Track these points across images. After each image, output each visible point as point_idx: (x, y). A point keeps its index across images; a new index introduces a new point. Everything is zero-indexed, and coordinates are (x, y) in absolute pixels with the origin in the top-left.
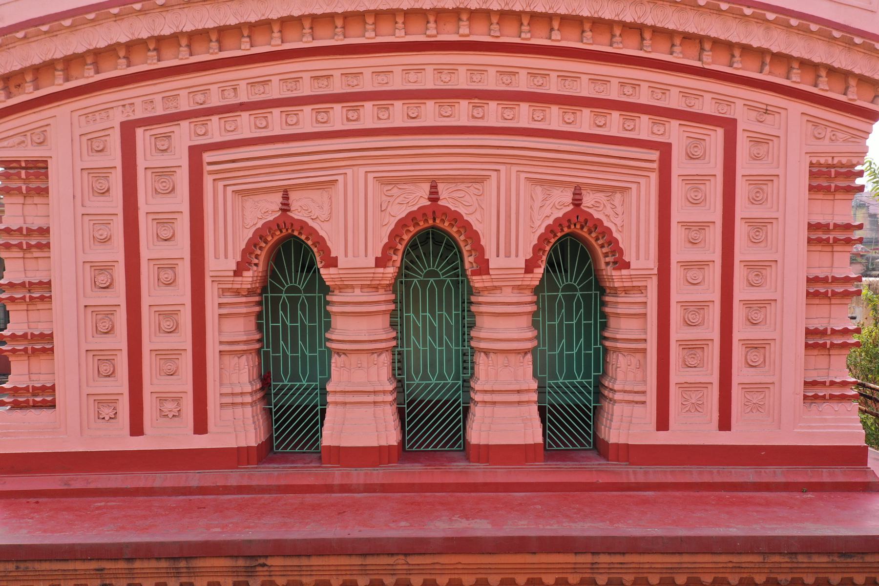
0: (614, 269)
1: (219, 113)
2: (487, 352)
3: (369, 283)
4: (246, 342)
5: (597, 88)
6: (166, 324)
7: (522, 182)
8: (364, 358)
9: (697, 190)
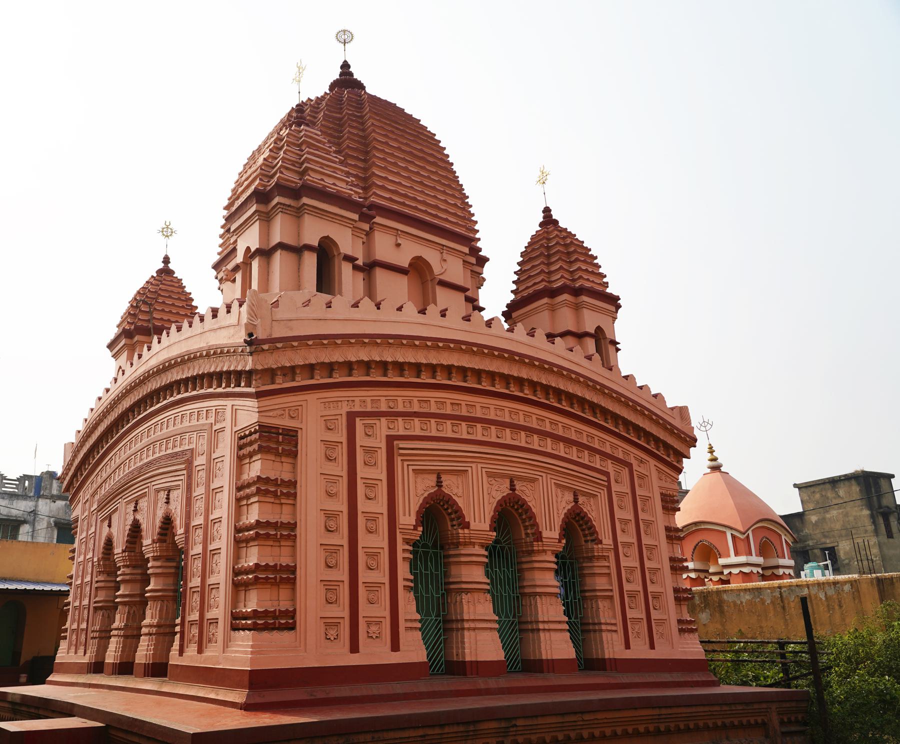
2: (540, 594)
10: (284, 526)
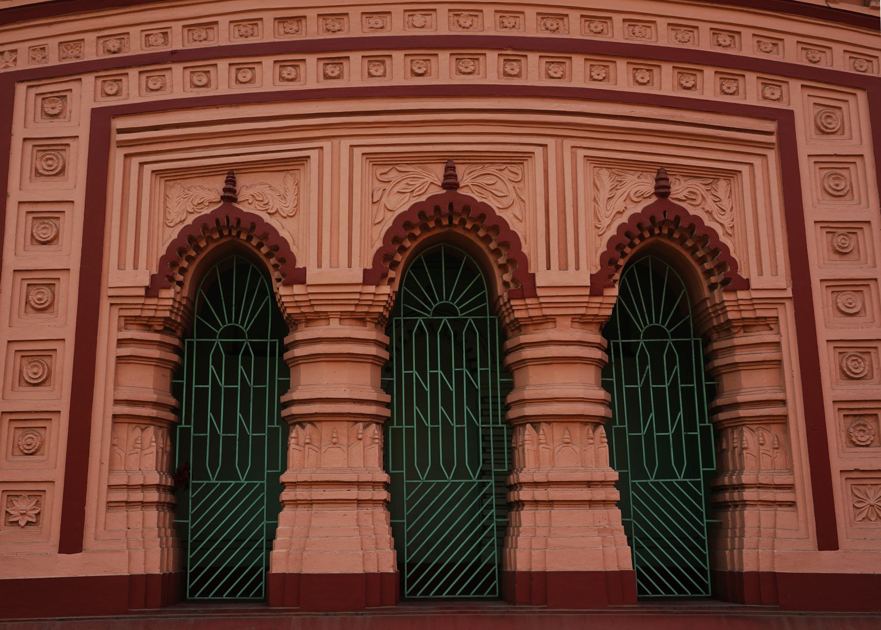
0: (726, 291)
1: (139, 66)
2: (536, 422)
3: (352, 309)
4: (155, 405)
5: (680, 36)
6: (29, 373)
7: (580, 161)
8: (343, 428)
9: (838, 177)
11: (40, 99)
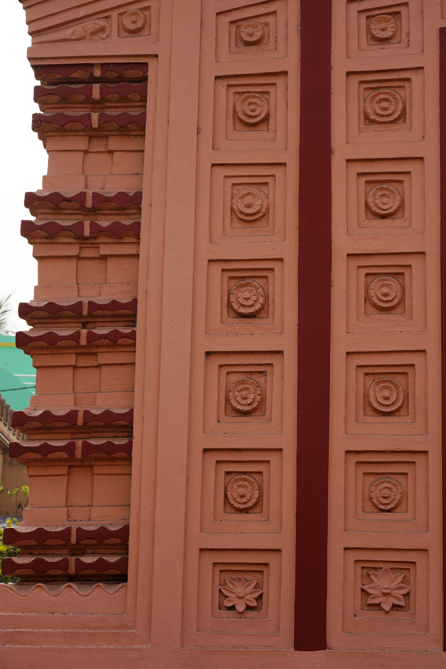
10: (97, 312)
11: (363, 17)
